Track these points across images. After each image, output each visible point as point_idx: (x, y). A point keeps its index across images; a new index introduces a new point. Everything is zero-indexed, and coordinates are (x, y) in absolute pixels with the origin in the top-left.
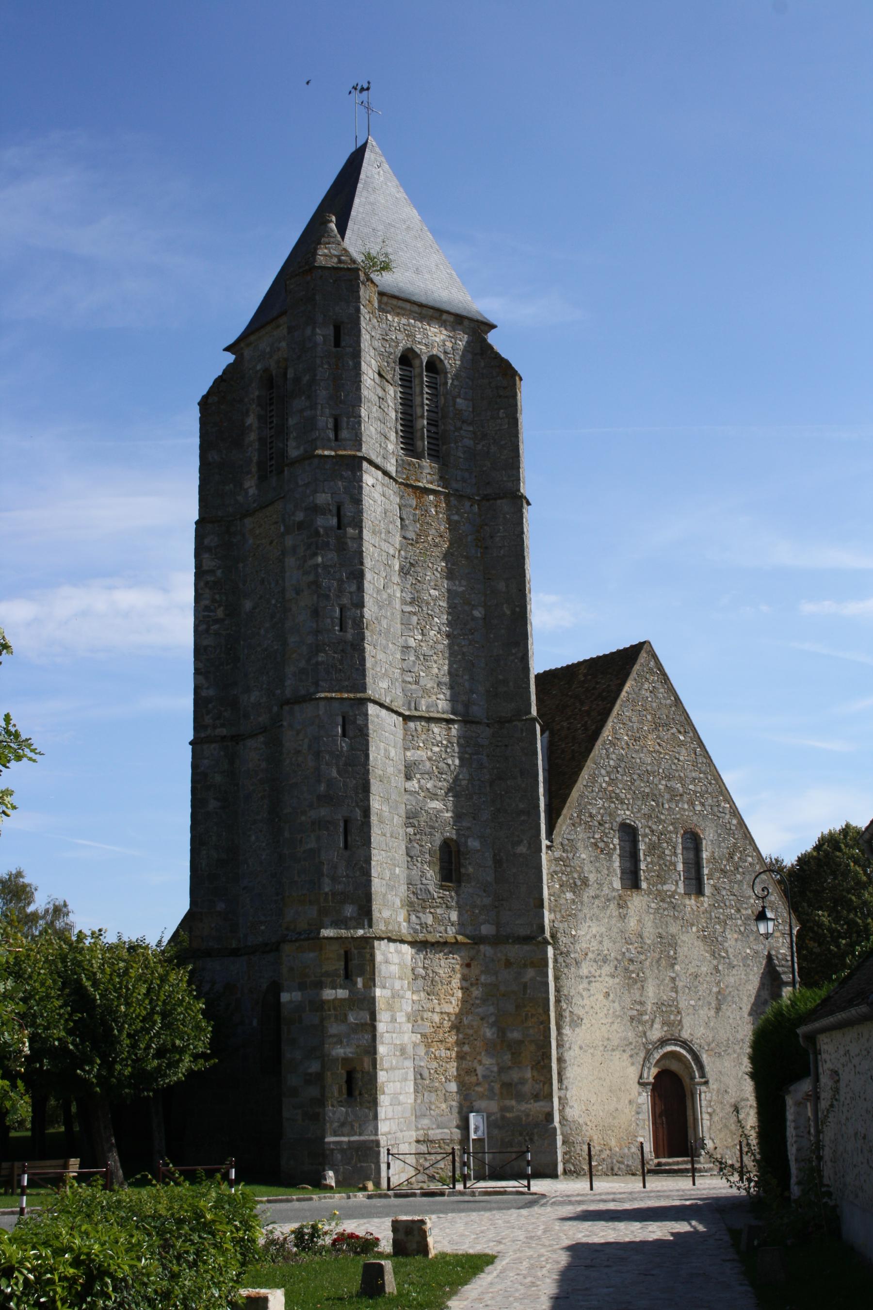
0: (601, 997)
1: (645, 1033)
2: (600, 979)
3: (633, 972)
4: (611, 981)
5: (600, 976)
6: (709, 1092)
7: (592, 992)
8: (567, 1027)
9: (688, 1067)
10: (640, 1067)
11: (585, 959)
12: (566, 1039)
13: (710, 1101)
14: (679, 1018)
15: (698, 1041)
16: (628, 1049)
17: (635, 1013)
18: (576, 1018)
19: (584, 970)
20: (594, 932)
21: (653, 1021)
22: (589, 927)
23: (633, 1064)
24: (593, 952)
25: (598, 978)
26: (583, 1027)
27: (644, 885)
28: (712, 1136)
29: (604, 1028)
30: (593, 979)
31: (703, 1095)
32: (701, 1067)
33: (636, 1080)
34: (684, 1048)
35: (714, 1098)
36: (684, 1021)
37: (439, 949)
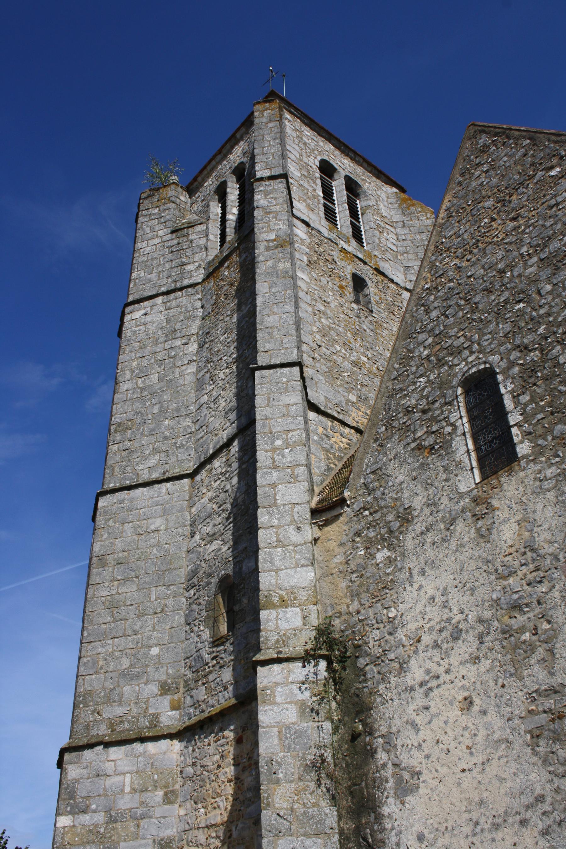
0: (454, 713)
2: (448, 677)
3: (522, 630)
4: (471, 671)
5: (447, 672)
7: (433, 710)
8: (391, 800)
11: (416, 652)
12: (388, 826)
16: (533, 816)
17: (543, 718)
18: (406, 776)
19: (416, 674)
20: (430, 592)
22: (421, 587)
24: (431, 629)
25: (445, 677)
26: (423, 790)
27: (524, 449)
29: (467, 780)
30: (434, 683)
37: (209, 730)
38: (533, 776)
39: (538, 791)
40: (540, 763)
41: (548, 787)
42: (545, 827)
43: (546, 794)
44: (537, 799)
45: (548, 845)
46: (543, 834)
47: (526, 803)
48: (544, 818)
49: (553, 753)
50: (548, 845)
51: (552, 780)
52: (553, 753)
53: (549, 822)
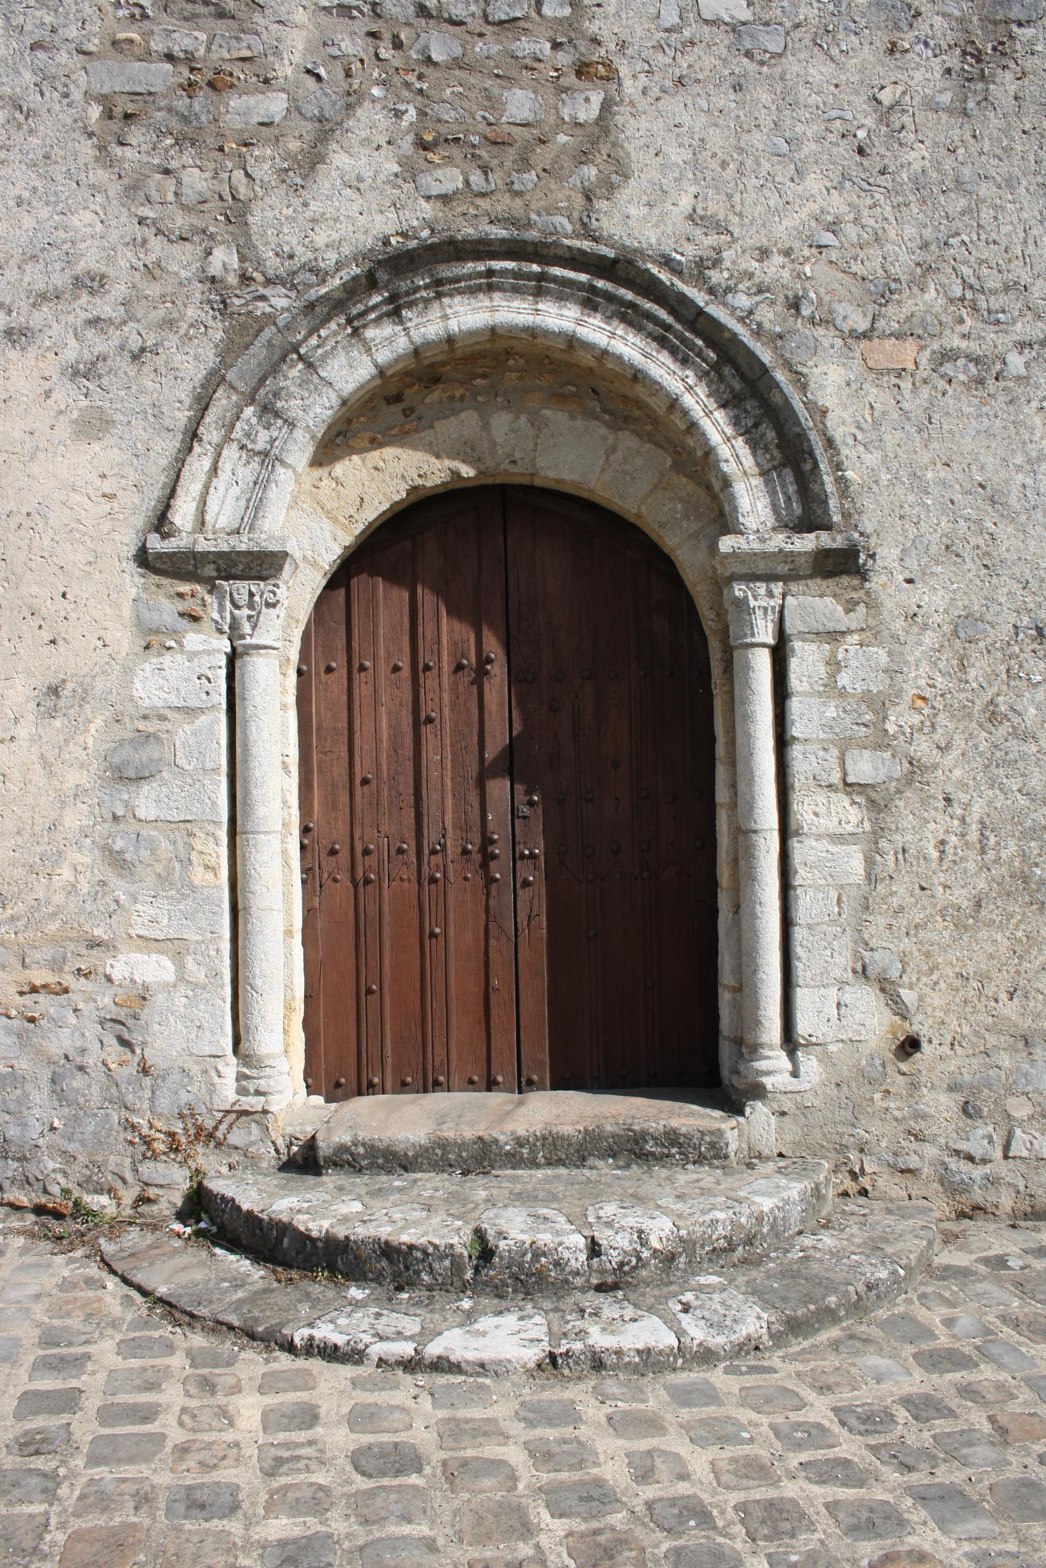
1: (236, 214)
6: (871, 634)
9: (697, 465)
10: (168, 446)
13: (879, 705)
14: (586, 106)
15: (775, 269)
17: (160, 76)
21: (326, 130)
23: (93, 426)
28: (879, 960)
31: (806, 663)
32: (791, 451)
33: (127, 541)
34: (629, 316)
35: (917, 677)
36: (635, 130)
38: (82, 220)
39: (90, 261)
40: (115, 189)
41: (126, 257)
42: (87, 356)
43: (111, 272)
44: (78, 282)
45: (84, 403)
46: (76, 373)
47: (40, 286)
48: (90, 334)
49: (167, 172)
50: (84, 403)
51: (145, 241)
52: (167, 172)
53: (99, 344)
